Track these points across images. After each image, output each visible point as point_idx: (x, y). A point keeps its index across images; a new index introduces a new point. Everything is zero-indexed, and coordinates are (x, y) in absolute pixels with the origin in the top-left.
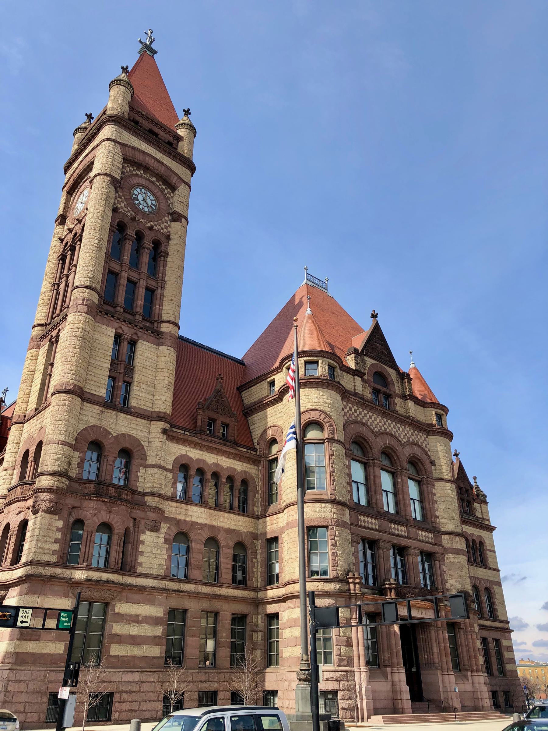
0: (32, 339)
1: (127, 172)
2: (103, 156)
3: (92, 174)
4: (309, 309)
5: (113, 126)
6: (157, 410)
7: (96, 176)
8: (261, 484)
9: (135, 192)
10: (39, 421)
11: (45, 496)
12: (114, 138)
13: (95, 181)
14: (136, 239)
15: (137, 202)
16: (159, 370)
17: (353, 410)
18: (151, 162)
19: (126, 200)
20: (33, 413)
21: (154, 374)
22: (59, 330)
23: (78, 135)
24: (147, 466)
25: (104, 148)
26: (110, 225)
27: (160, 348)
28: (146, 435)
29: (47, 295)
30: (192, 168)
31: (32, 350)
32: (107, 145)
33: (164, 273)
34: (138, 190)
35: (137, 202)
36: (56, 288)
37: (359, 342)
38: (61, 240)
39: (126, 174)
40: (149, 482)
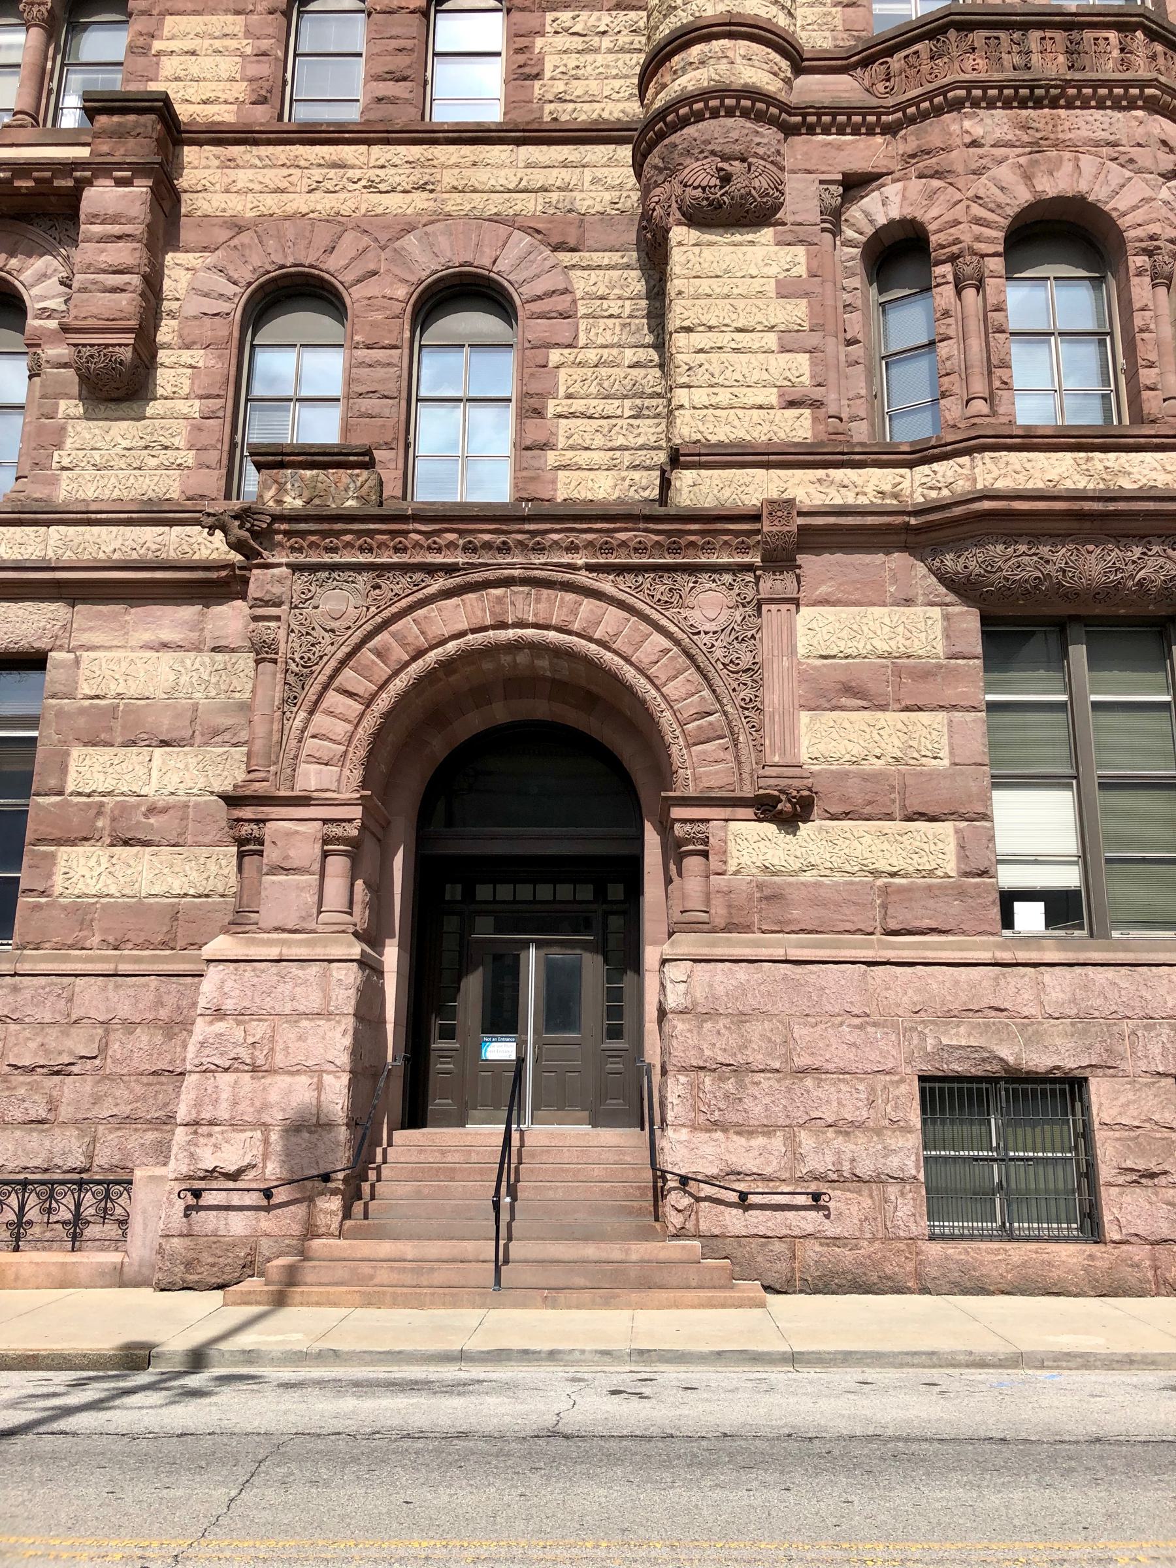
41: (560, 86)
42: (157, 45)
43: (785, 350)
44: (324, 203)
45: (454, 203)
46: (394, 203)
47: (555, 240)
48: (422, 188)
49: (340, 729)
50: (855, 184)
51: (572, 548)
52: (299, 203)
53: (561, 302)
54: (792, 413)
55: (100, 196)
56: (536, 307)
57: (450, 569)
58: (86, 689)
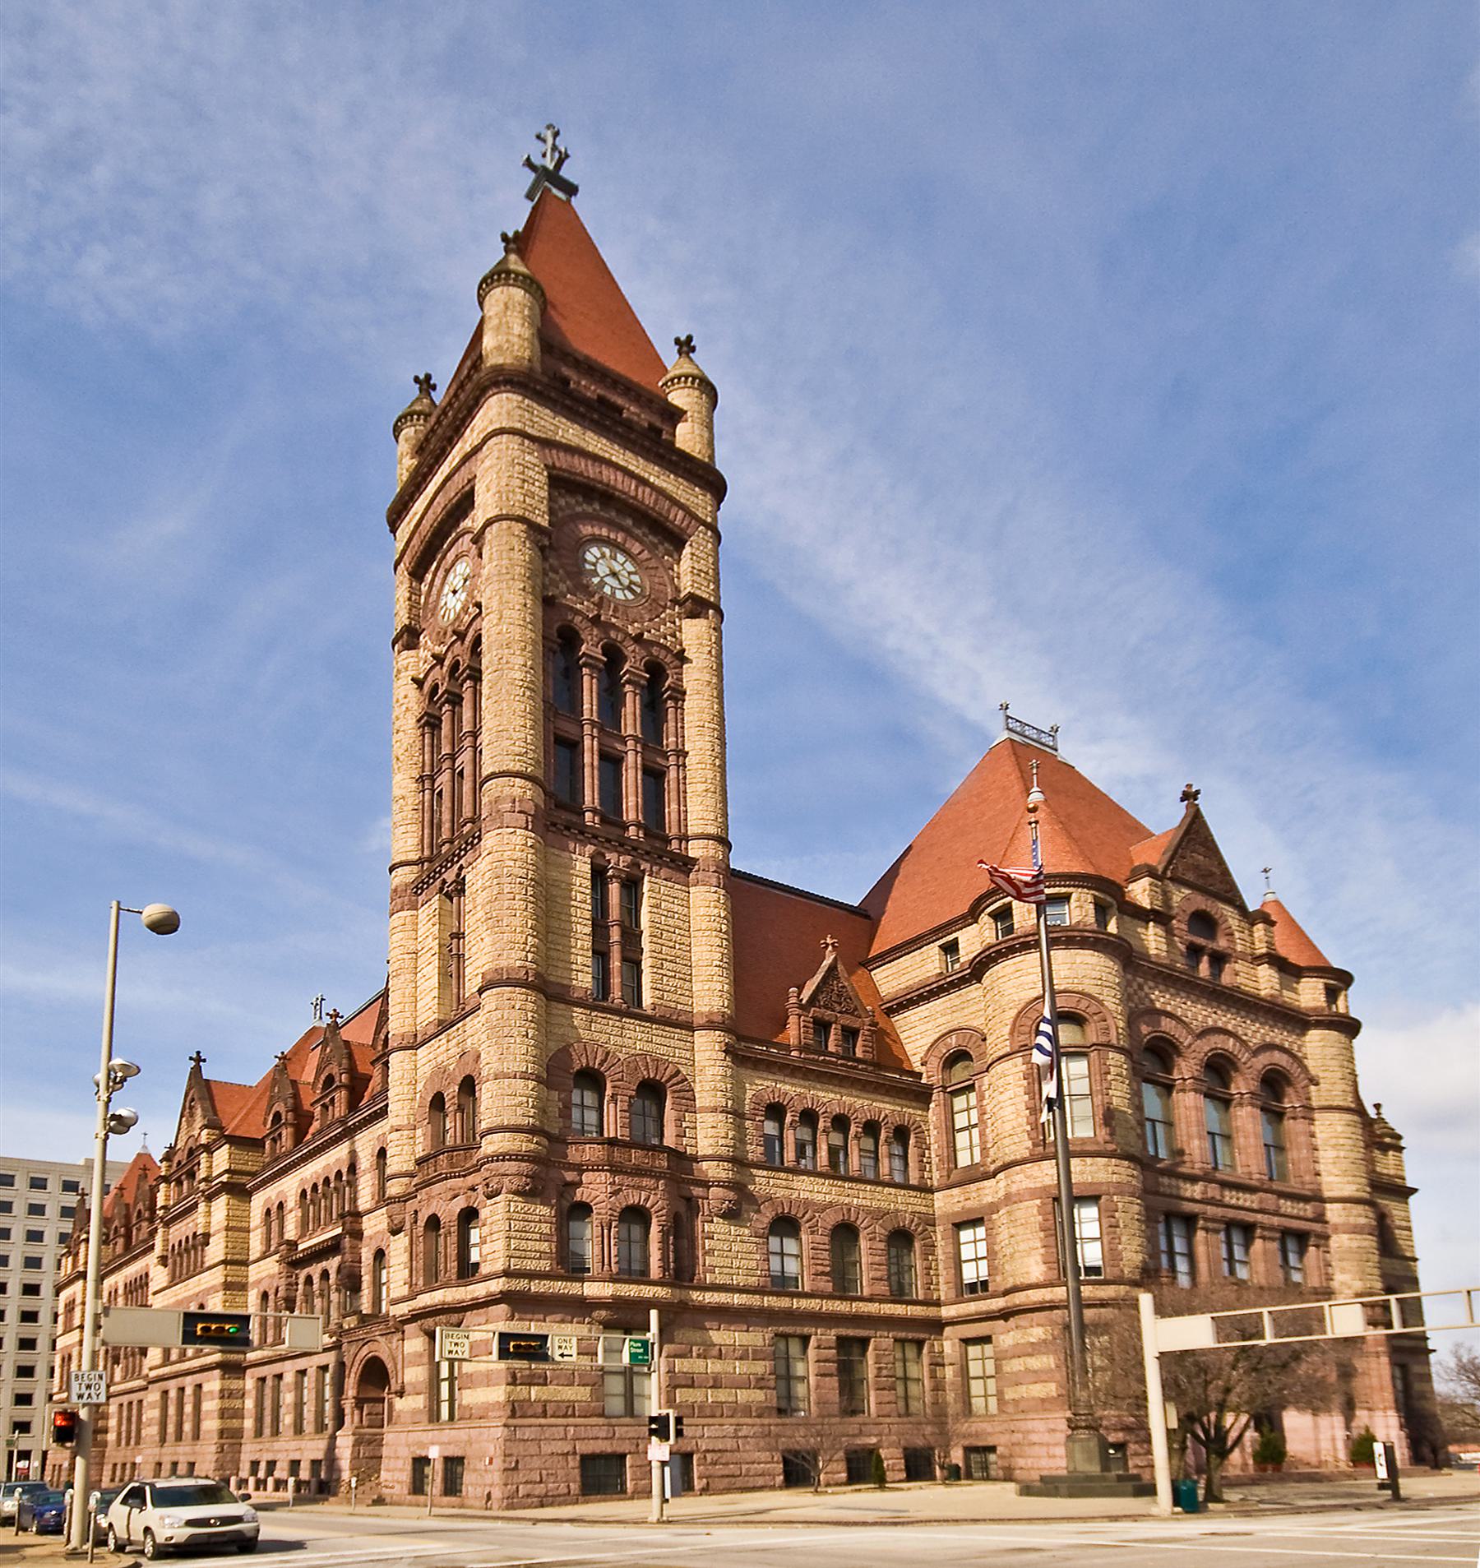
1: (561, 508)
2: (500, 470)
3: (475, 520)
4: (1036, 789)
5: (510, 395)
9: (589, 557)
12: (519, 426)
13: (488, 536)
14: (605, 664)
15: (596, 580)
17: (1135, 986)
19: (568, 574)
23: (408, 432)
25: (496, 454)
26: (544, 637)
30: (716, 487)
32: (504, 446)
34: (594, 550)
35: (596, 580)
37: (1152, 854)
39: (560, 514)
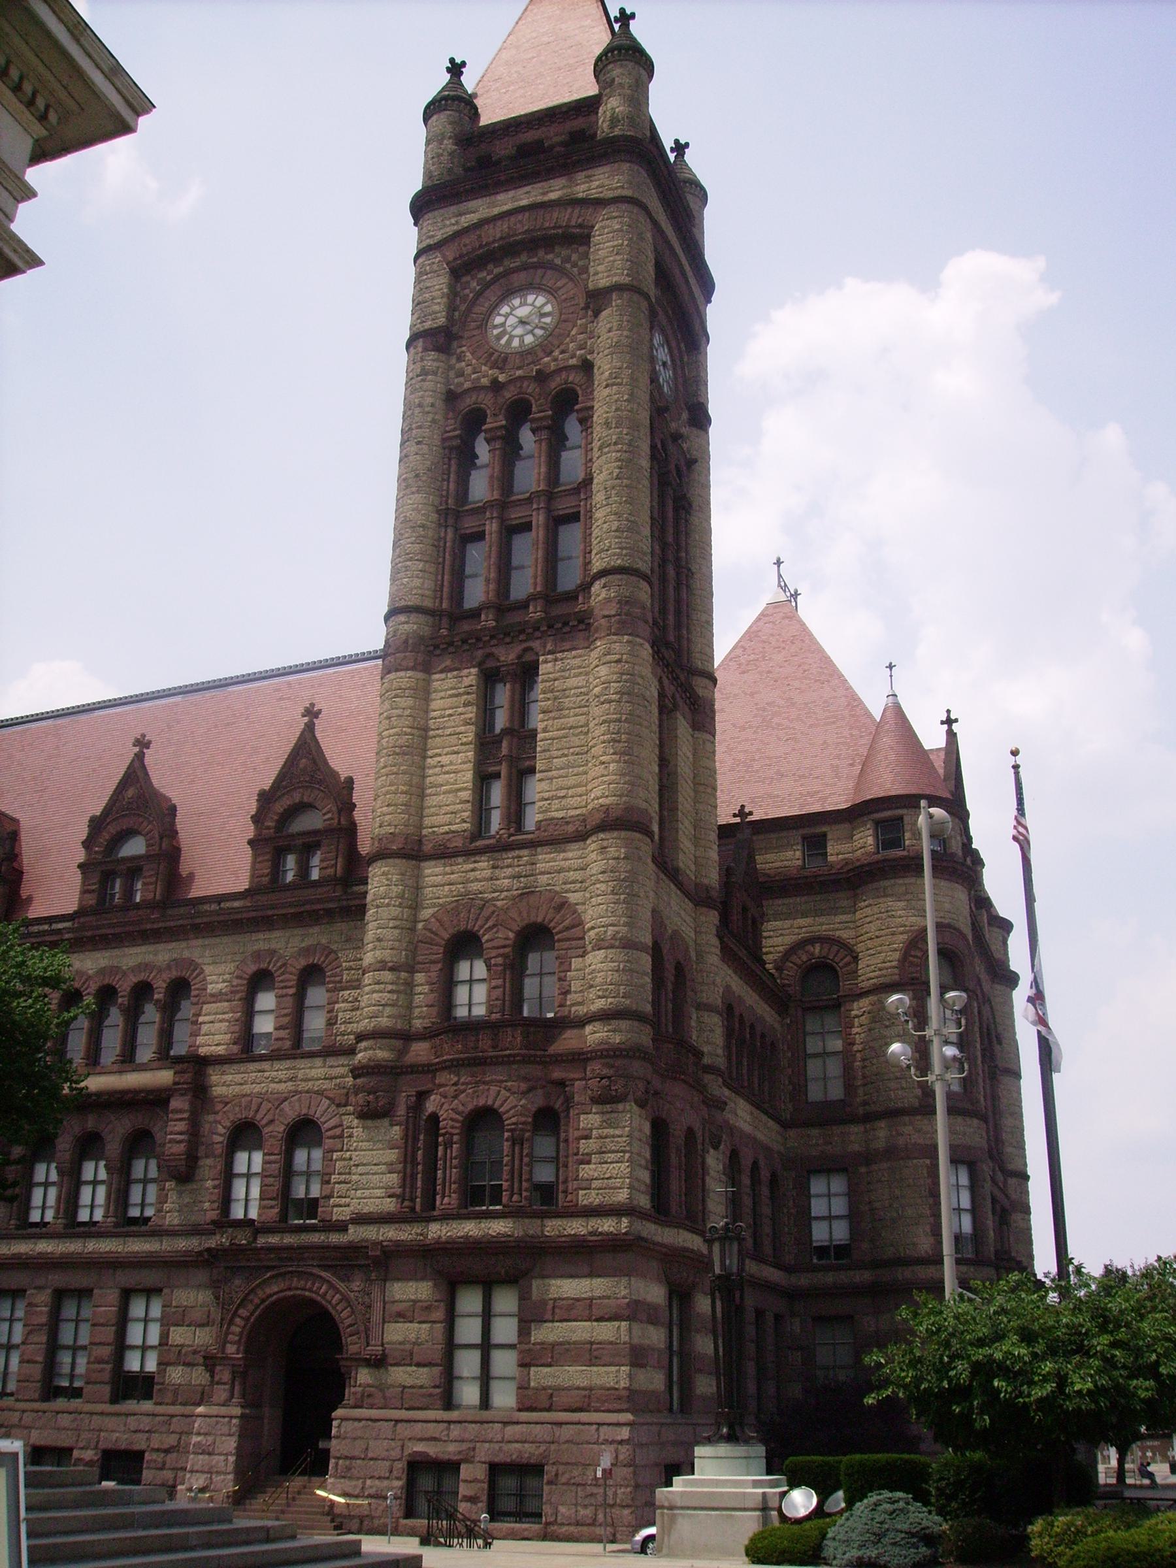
0: (406, 642)
6: (706, 881)
7: (618, 288)
8: (790, 1054)
10: (509, 871)
11: (638, 1068)
16: (701, 788)
18: (677, 271)
20: (458, 843)
21: (692, 794)
22: (526, 650)
24: (700, 1007)
27: (697, 734)
28: (692, 935)
29: (430, 534)
31: (409, 673)
33: (687, 553)
36: (451, 521)
38: (451, 397)
40: (708, 1043)
41: (343, 1028)
42: (201, 1019)
43: (390, 1173)
44: (257, 1088)
45: (303, 1086)
46: (282, 1087)
47: (337, 1102)
48: (291, 1080)
49: (238, 1330)
50: (422, 1096)
51: (313, 1259)
52: (247, 1089)
53: (338, 1131)
54: (389, 1200)
55: (175, 1103)
56: (329, 1133)
57: (274, 1267)
58: (174, 1304)
